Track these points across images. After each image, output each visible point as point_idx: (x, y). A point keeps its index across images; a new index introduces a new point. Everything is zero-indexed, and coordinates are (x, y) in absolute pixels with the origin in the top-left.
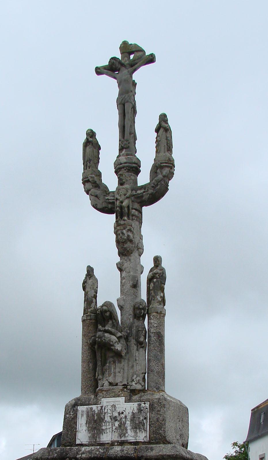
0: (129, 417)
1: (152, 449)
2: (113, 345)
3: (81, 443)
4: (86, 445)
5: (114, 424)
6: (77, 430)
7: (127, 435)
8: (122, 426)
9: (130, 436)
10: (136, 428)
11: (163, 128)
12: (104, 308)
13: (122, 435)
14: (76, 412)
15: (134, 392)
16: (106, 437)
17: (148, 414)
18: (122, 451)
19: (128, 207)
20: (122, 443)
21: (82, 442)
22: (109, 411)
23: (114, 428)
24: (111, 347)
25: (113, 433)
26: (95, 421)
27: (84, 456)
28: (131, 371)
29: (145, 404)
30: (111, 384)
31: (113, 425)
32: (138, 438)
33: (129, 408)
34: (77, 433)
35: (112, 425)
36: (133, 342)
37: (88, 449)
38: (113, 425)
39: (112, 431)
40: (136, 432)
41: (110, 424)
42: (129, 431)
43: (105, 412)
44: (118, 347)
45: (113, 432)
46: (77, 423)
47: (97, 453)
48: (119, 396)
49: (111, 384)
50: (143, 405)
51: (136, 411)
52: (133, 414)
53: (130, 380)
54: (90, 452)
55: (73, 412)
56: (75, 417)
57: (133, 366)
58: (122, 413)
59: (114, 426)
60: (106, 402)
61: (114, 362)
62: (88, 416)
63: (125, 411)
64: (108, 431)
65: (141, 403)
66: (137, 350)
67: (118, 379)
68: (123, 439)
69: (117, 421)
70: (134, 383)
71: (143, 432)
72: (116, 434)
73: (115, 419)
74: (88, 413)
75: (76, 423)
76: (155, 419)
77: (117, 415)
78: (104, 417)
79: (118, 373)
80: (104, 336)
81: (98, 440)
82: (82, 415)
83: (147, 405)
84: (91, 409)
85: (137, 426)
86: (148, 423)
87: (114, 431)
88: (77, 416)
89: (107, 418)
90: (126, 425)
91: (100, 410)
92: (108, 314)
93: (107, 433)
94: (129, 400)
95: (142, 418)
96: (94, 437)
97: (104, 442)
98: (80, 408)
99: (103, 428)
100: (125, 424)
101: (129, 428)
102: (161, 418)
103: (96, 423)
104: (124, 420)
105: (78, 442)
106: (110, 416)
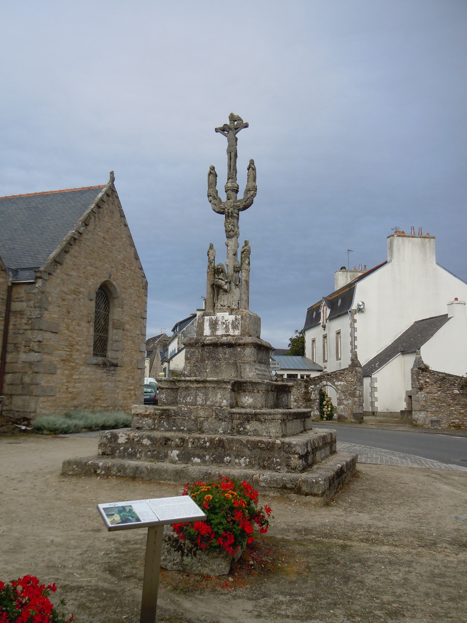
4: (209, 336)
8: (227, 327)
9: (231, 332)
11: (251, 167)
12: (219, 267)
14: (204, 319)
15: (232, 310)
16: (220, 332)
18: (227, 339)
19: (232, 212)
26: (213, 324)
27: (208, 342)
33: (231, 318)
36: (233, 284)
37: (210, 338)
38: (223, 326)
40: (234, 330)
44: (226, 287)
50: (238, 317)
51: (234, 320)
52: (233, 321)
54: (211, 340)
56: (203, 322)
57: (233, 297)
60: (219, 315)
62: (210, 321)
67: (226, 303)
73: (224, 323)
74: (210, 320)
75: (203, 325)
82: (207, 321)
83: (240, 317)
85: (235, 327)
89: (220, 323)
92: (221, 270)
94: (231, 314)
100: (228, 326)
101: (230, 328)
103: (214, 325)
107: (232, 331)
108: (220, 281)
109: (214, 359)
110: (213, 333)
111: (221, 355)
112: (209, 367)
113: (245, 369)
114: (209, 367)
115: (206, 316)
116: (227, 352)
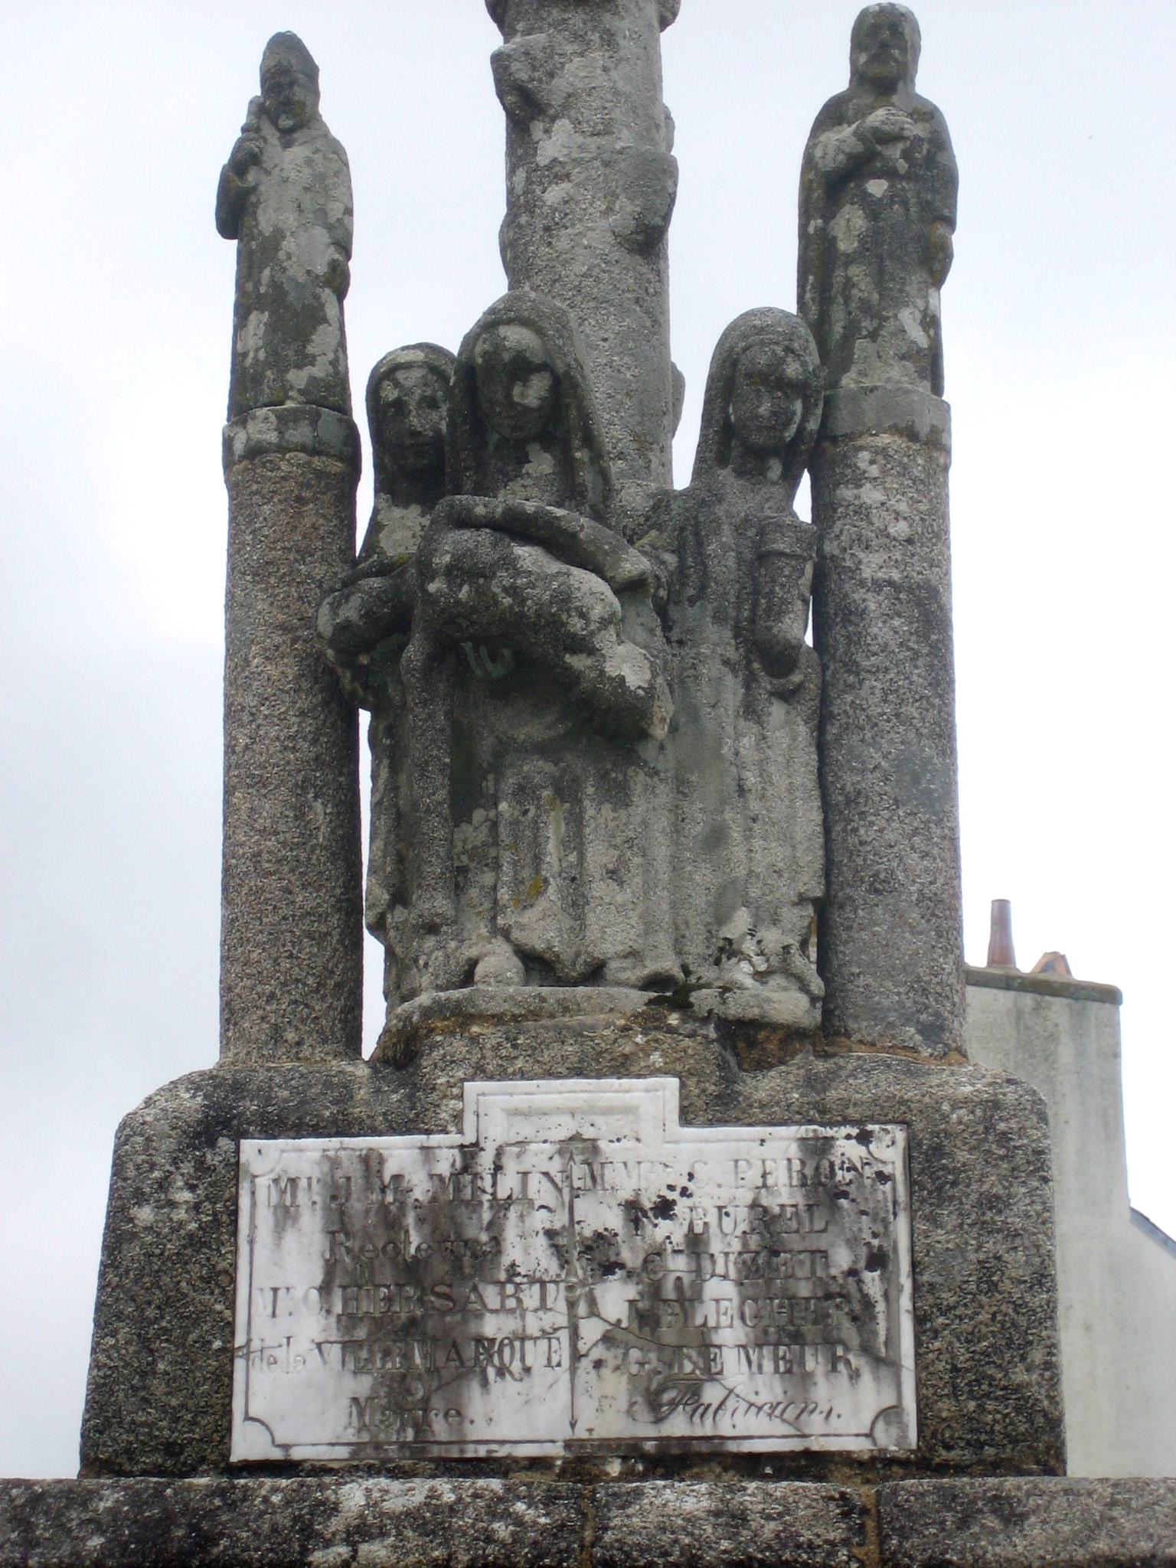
0: (726, 1244)
1: (1012, 1516)
2: (583, 645)
3: (277, 1454)
5: (592, 1302)
6: (240, 1340)
7: (711, 1394)
8: (663, 1322)
9: (746, 1402)
10: (797, 1338)
12: (515, 336)
13: (667, 1397)
14: (221, 1191)
15: (747, 1041)
16: (529, 1407)
17: (901, 1228)
20: (675, 1461)
21: (286, 1447)
22: (540, 1191)
23: (591, 1331)
24: (568, 658)
25: (580, 1372)
26: (412, 1271)
28: (703, 876)
29: (864, 1138)
30: (537, 964)
31: (582, 1309)
32: (815, 1423)
34: (239, 1364)
35: (572, 1305)
36: (716, 643)
39: (576, 1356)
40: (795, 1375)
41: (557, 1297)
42: (733, 1366)
43: (502, 1194)
44: (627, 663)
45: (586, 1364)
46: (233, 1281)
47: (502, 1530)
48: (622, 1067)
49: (537, 964)
51: (784, 1194)
52: (764, 1219)
53: (696, 947)
55: (192, 1188)
56: (220, 1225)
57: (716, 838)
58: (664, 1209)
59: (594, 1312)
60: (513, 1114)
61: (567, 792)
62: (338, 1224)
63: (685, 1193)
64: (535, 1354)
65: (829, 1132)
66: (750, 710)
67: (611, 931)
68: (678, 1426)
69: (619, 1273)
70: (741, 972)
71: (867, 1377)
72: (616, 1386)
73: (599, 1256)
74: (336, 1195)
75: (222, 1282)
76: (964, 1270)
77: (613, 1220)
78: (497, 1241)
79: (614, 881)
80: (510, 563)
81: (440, 1429)
82: (286, 1215)
83: (889, 1150)
84: (371, 1163)
85: (806, 1321)
86: (905, 1302)
87: (598, 1352)
88: (235, 1223)
89: (524, 1248)
90: (706, 1312)
91: (455, 1175)
92: (533, 393)
93: (527, 1370)
94: (711, 1105)
95: (842, 1258)
96: (399, 1399)
97: (502, 1452)
98: (266, 1158)
99: (492, 1326)
100: (688, 1298)
101: (730, 1335)
102: (1017, 1262)
103: (417, 1287)
104: (679, 1265)
105: (247, 1444)
106: (550, 1234)
107: (769, 1388)
108: (527, 555)
110: (408, 1427)
115: (274, 1126)
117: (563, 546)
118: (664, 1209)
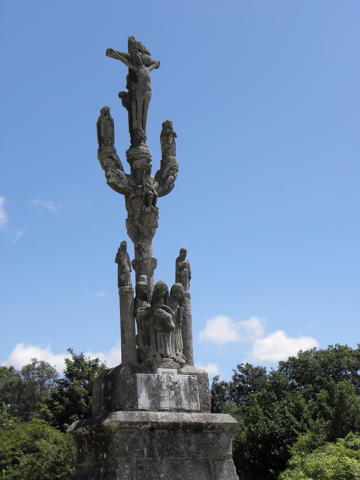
3: (143, 408)
5: (171, 393)
6: (138, 396)
7: (182, 403)
13: (178, 403)
21: (144, 407)
22: (165, 381)
23: (171, 396)
25: (170, 401)
29: (194, 377)
31: (170, 394)
34: (138, 398)
35: (169, 393)
38: (170, 393)
39: (170, 399)
40: (190, 402)
43: (162, 381)
45: (171, 400)
46: (137, 389)
48: (172, 368)
55: (132, 379)
59: (171, 394)
63: (178, 382)
64: (166, 398)
65: (190, 376)
68: (179, 407)
69: (173, 390)
71: (195, 402)
72: (174, 402)
78: (162, 386)
87: (171, 399)
88: (136, 383)
89: (164, 387)
91: (157, 378)
93: (165, 400)
96: (153, 402)
97: (164, 409)
100: (179, 393)
101: (183, 397)
105: (140, 407)
106: (166, 385)
109: (172, 454)
111: (182, 447)
112: (164, 469)
113: (221, 471)
114: (164, 469)
116: (193, 441)
117: (168, 311)
118: (176, 383)
